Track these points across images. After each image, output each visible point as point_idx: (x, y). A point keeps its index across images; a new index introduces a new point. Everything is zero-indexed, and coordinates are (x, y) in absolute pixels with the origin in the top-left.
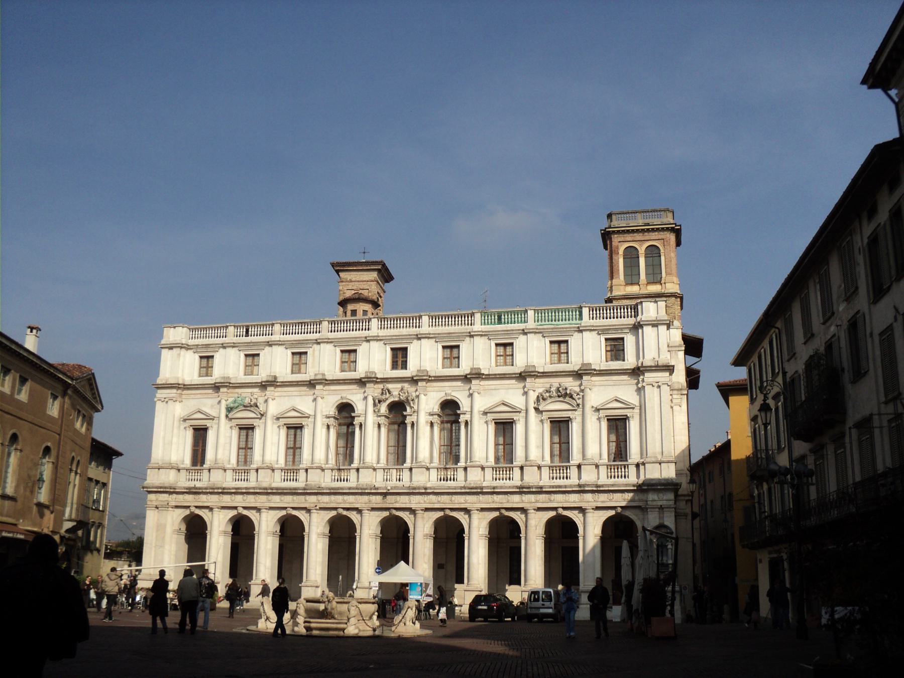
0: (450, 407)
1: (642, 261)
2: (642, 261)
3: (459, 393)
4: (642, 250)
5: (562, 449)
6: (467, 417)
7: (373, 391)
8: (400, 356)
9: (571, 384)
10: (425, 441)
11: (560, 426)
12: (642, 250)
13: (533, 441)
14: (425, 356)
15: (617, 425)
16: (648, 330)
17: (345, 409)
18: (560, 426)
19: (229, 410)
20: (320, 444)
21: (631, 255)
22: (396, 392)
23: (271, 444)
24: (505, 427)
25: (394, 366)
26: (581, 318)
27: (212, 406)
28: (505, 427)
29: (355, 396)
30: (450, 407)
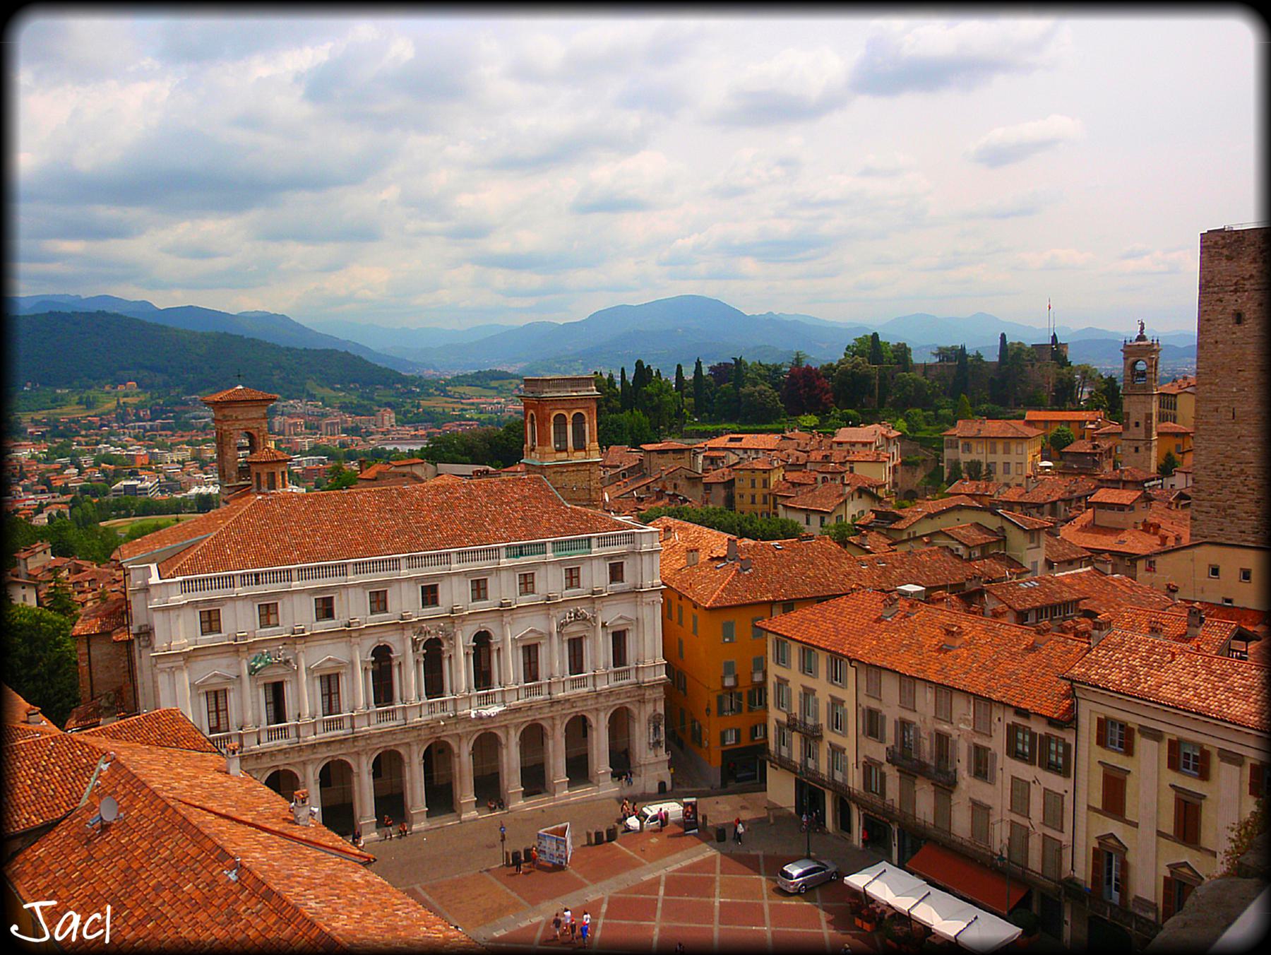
0: (482, 640)
1: (570, 428)
2: (570, 428)
3: (491, 626)
4: (570, 420)
5: (576, 664)
6: (500, 645)
7: (410, 635)
8: (430, 595)
9: (584, 609)
10: (460, 672)
11: (576, 646)
12: (570, 420)
13: (554, 659)
14: (455, 595)
15: (619, 639)
16: (646, 558)
17: (382, 656)
18: (576, 646)
19: (253, 671)
20: (358, 689)
21: (560, 421)
22: (433, 631)
23: (304, 699)
24: (530, 652)
25: (425, 603)
26: (590, 547)
27: (228, 666)
28: (530, 652)
29: (392, 639)
30: (482, 640)
